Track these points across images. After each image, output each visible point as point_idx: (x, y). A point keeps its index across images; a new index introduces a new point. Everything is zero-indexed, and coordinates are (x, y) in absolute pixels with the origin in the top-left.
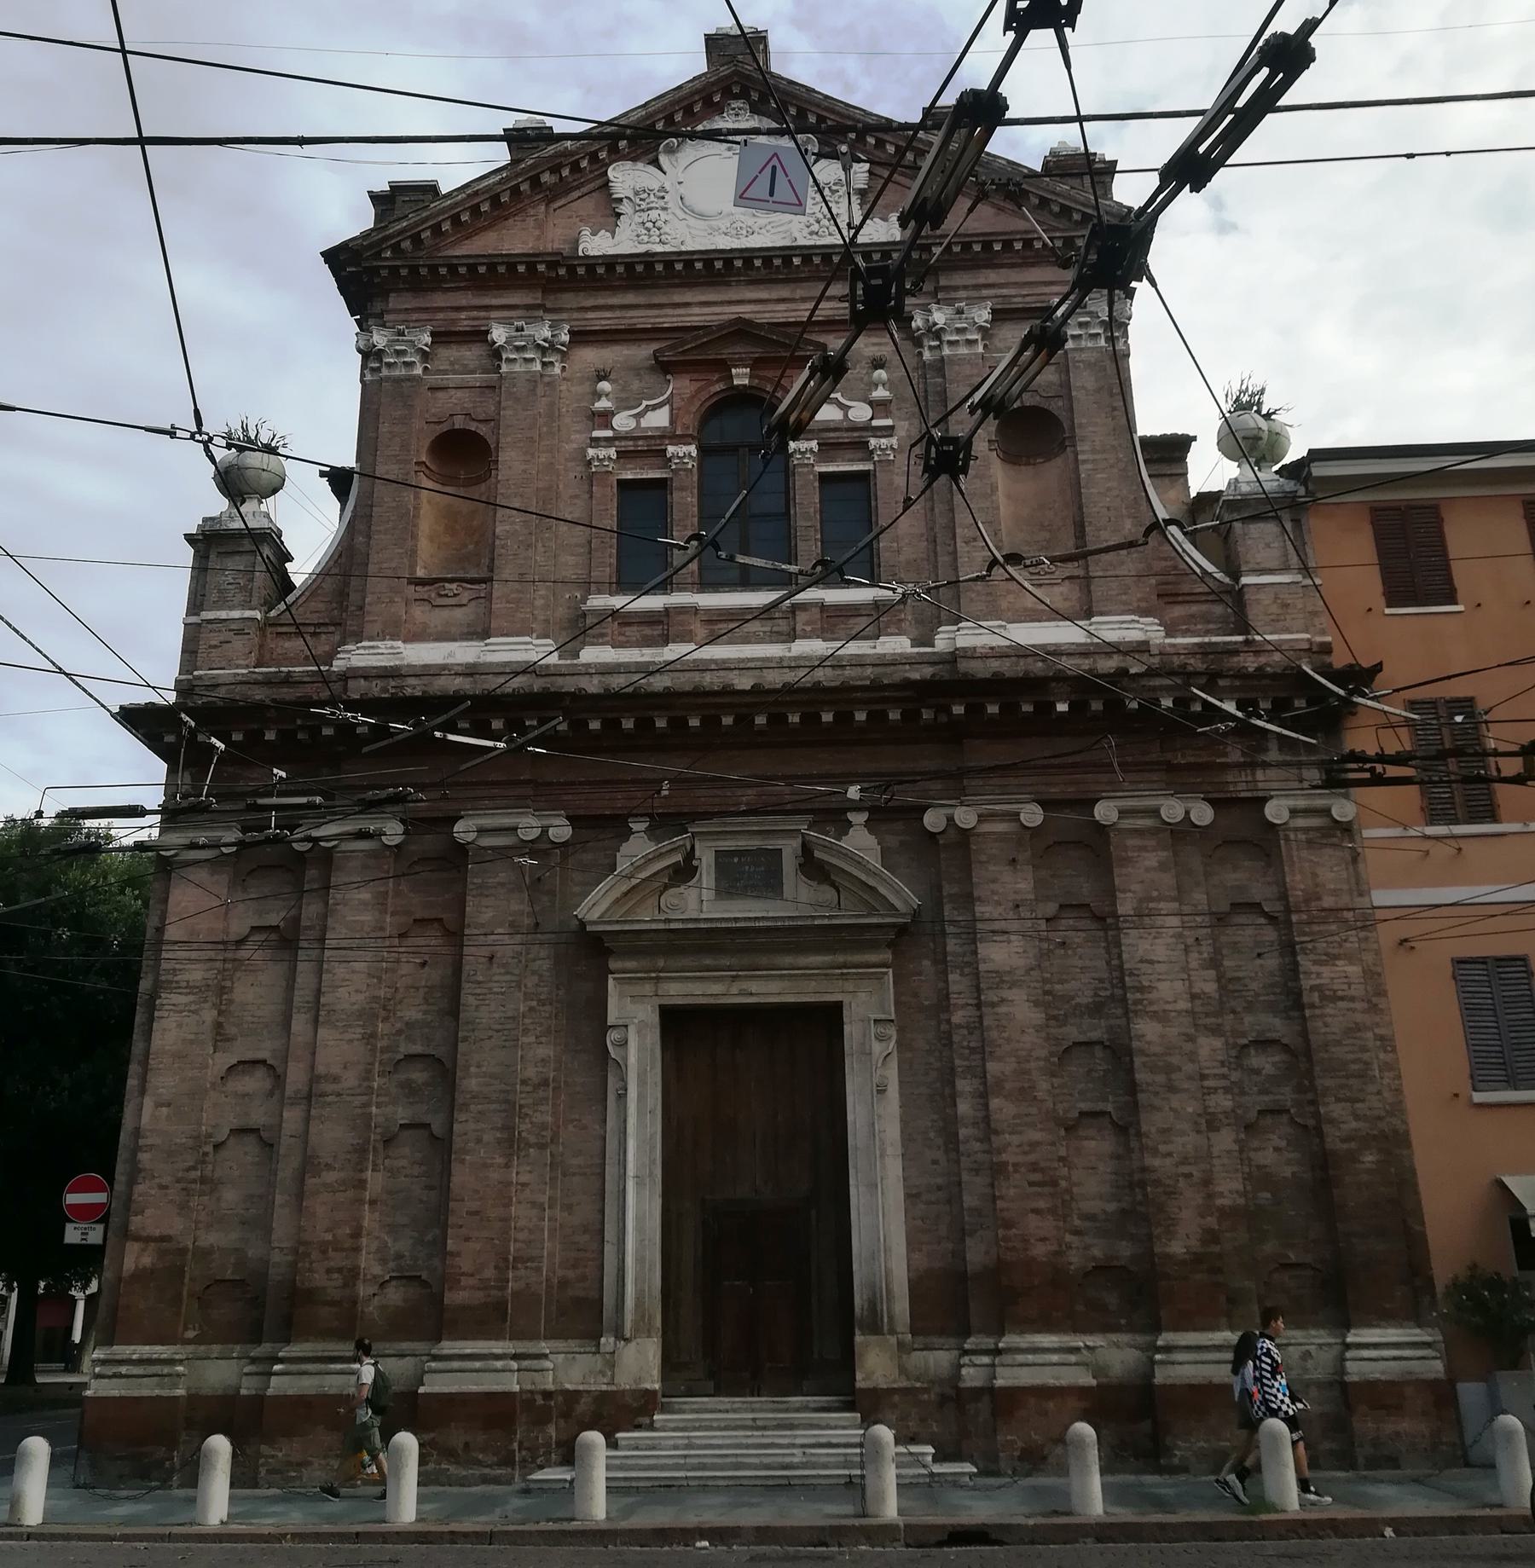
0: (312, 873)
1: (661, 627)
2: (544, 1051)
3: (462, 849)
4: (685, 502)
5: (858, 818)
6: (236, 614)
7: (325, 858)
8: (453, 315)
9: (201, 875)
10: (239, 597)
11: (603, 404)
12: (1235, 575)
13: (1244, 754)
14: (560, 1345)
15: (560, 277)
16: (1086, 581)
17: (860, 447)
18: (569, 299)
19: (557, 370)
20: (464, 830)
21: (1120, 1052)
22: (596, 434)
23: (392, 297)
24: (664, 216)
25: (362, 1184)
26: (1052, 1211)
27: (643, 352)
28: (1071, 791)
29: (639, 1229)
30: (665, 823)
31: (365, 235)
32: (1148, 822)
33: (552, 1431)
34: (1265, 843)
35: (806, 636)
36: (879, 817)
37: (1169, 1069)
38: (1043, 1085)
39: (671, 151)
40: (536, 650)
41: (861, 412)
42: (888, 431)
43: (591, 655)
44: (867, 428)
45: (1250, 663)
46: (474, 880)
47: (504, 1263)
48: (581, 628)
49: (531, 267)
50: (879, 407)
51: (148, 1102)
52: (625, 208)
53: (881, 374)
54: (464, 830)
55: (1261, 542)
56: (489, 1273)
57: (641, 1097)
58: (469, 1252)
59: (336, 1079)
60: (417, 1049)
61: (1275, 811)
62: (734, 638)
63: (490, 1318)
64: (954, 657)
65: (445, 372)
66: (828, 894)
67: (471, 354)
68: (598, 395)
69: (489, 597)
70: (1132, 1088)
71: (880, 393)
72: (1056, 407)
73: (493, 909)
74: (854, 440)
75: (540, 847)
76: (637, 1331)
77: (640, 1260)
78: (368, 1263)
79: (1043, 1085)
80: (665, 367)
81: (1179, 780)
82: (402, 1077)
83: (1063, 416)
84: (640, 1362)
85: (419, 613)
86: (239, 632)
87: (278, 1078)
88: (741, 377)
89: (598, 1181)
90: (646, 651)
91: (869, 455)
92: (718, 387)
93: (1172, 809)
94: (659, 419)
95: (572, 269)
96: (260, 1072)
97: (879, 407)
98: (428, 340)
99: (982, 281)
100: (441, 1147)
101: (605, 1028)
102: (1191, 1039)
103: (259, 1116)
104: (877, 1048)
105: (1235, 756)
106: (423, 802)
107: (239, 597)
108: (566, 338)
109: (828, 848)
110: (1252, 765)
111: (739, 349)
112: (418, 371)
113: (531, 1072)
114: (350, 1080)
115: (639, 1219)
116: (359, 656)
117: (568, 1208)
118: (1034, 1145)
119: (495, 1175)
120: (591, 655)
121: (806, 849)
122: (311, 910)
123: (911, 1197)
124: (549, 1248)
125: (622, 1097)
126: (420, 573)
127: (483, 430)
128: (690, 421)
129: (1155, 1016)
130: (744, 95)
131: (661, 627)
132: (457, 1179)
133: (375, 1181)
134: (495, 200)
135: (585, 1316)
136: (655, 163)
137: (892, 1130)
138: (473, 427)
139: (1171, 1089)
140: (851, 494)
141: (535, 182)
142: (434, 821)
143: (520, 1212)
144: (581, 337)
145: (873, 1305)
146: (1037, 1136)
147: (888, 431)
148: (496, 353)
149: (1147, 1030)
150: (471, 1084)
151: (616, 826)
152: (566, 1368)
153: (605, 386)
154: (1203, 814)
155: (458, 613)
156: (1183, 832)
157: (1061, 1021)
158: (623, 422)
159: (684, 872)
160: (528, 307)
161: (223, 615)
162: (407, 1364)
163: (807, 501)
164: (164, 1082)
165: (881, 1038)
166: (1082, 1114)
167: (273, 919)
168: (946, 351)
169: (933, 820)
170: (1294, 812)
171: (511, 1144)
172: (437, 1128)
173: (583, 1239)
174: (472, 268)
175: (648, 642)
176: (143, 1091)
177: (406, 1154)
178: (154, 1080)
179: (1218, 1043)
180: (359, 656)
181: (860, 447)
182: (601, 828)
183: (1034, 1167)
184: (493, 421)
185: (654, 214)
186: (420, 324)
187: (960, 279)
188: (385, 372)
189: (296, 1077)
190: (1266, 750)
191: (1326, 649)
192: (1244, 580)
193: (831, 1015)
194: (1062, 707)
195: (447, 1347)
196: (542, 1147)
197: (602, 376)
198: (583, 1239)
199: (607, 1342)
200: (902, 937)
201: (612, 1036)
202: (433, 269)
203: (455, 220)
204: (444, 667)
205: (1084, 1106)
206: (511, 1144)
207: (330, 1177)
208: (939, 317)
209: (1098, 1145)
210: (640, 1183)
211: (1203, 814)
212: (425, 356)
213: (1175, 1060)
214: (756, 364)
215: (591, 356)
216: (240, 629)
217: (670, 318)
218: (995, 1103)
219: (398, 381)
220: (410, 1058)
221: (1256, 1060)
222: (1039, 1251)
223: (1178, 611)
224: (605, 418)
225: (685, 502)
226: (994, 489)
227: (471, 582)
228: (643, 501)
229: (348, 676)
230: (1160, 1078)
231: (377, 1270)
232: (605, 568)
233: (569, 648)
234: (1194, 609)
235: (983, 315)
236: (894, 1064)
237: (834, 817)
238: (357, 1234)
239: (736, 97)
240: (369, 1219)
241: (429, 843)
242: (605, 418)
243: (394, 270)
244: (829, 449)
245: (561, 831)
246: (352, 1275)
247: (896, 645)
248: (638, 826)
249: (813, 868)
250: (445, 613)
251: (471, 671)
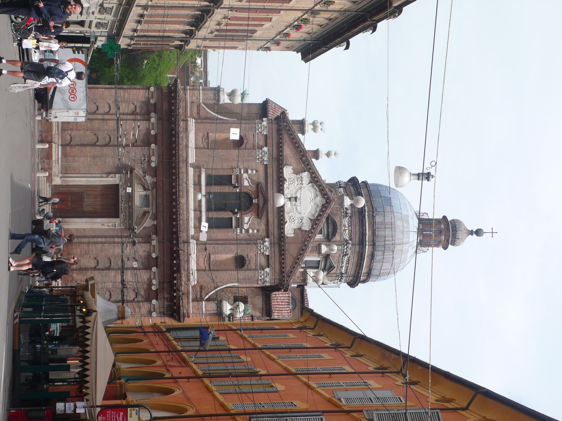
0: (146, 117)
1: (198, 184)
2: (111, 162)
3: (149, 146)
4: (227, 189)
5: (155, 223)
6: (201, 97)
7: (149, 120)
8: (271, 139)
9: (147, 95)
10: (205, 98)
11: (250, 171)
12: (205, 301)
13: (167, 298)
14: (60, 167)
15: (280, 163)
16: (204, 270)
17: (238, 226)
18: (275, 164)
19: (258, 161)
20: (153, 146)
21: (109, 268)
22: (242, 170)
23: (276, 125)
24: (296, 185)
25: (87, 130)
26: (81, 254)
27: (262, 180)
28: (159, 263)
29: (79, 181)
30: (155, 184)
31: (288, 119)
32: (152, 277)
33: (46, 166)
34: (148, 300)
35: (194, 213)
36: (155, 227)
37: (106, 276)
38: (104, 254)
39: (313, 186)
40: (192, 159)
41: (246, 226)
42: (241, 232)
43: (191, 171)
44: (242, 228)
45: (185, 301)
46: (143, 148)
47: (74, 156)
48: (197, 168)
49: (281, 156)
50: (247, 231)
51: (103, 90)
52: (298, 176)
53: (256, 231)
54: (153, 146)
55: (212, 306)
56: (72, 154)
57: (102, 181)
58: (75, 150)
59: (107, 124)
60: (112, 139)
61: (154, 302)
62: (194, 197)
63: (65, 155)
64: (188, 242)
65: (258, 137)
66: (140, 217)
67: (262, 143)
68: (252, 170)
69: (204, 148)
70: (102, 270)
71: (251, 231)
72: (246, 267)
73: (138, 153)
74: (239, 224)
75: (149, 161)
76: (62, 180)
77: (74, 181)
78: (73, 133)
79: (104, 254)
80: (258, 185)
81: (161, 283)
82: (107, 136)
83: (244, 268)
84: (57, 181)
85: (202, 134)
86: (197, 98)
87: (107, 113)
88: (255, 201)
89: (88, 174)
90: (192, 181)
91: (236, 228)
92: (253, 197)
93: (154, 282)
94: (246, 183)
95: (281, 164)
96: (108, 110)
97: (247, 231)
98: (265, 134)
99: (276, 254)
100: (94, 145)
101: (115, 173)
102: (111, 282)
103: (101, 111)
104: (111, 224)
105: (166, 296)
106: (159, 138)
107: (205, 98)
108: (265, 163)
109: (148, 216)
110: (164, 299)
111: (261, 201)
112: (257, 132)
113: (107, 160)
114: (106, 127)
115: (81, 180)
116: (192, 123)
117: (83, 168)
118: (93, 251)
119: (89, 154)
120: (191, 171)
121: (149, 212)
122: (139, 117)
123: (84, 230)
124: (76, 165)
125: (102, 177)
126: (210, 135)
127: (243, 146)
128: (245, 190)
129: (116, 275)
130: (327, 203)
131: (198, 184)
132: (88, 147)
133: (88, 133)
134: (299, 147)
135: (65, 171)
136: (310, 182)
137: (96, 226)
138: (244, 144)
139: (102, 277)
140: (227, 224)
141: (303, 156)
142: (156, 140)
143: (82, 159)
144: (266, 166)
145: (66, 222)
146: (94, 252)
147: (241, 232)
148: (261, 149)
149: (112, 273)
150: (105, 149)
151: (155, 175)
152: (56, 168)
153: (254, 172)
154: (154, 288)
155: (201, 142)
156: (150, 284)
157: (115, 259)
158: (245, 176)
159: (145, 189)
160: (272, 155)
161: (201, 95)
162: (57, 141)
163: (226, 215)
164: (107, 92)
165: (112, 225)
166: (98, 261)
167: (138, 110)
168: (259, 245)
169: (154, 237)
170: (154, 305)
171: (94, 157)
172: (97, 144)
173: (78, 170)
174: (281, 143)
175: (194, 182)
176: (105, 88)
177: (94, 139)
178: (107, 90)
179: (111, 287)
180: (192, 123)
181: (238, 226)
182: (154, 172)
183: (89, 251)
184: (245, 149)
185: (296, 182)
186: (269, 131)
187: (277, 249)
188: (257, 124)
189: (107, 117)
190: (167, 301)
191: (189, 317)
192: (204, 302)
193: (117, 216)
194: (175, 262)
195: (60, 147)
196: (94, 163)
197: (256, 171)
198: (78, 170)
199: (60, 175)
200: (131, 229)
201: (114, 175)
202: (281, 134)
203: (294, 139)
204: (188, 141)
205: (99, 262)
206: (94, 157)
207: (89, 125)
208: (267, 244)
209: (93, 264)
210: (87, 181)
211: (154, 288)
212: (261, 133)
213: (107, 278)
214: (258, 204)
215: (261, 169)
216: (198, 99)
217: (269, 185)
218: (100, 245)
219: (255, 127)
220: (110, 138)
221: (108, 293)
222: (75, 251)
223: (199, 289)
224: (247, 172)
225: (227, 189)
226: (227, 254)
227: (208, 145)
228: (225, 180)
229: (187, 121)
230: (104, 275)
231: (73, 134)
232: (210, 172)
233: (192, 165)
234: (199, 292)
235: (267, 254)
236: (108, 227)
237: (155, 217)
238: (79, 130)
239: (326, 201)
240: (82, 132)
241: (152, 139)
242: (247, 172)
243: (281, 126)
244: (237, 219)
245: (153, 165)
246: (72, 130)
247: (192, 232)
248: (155, 180)
249: (145, 213)
250: (201, 140)
251: (187, 146)
